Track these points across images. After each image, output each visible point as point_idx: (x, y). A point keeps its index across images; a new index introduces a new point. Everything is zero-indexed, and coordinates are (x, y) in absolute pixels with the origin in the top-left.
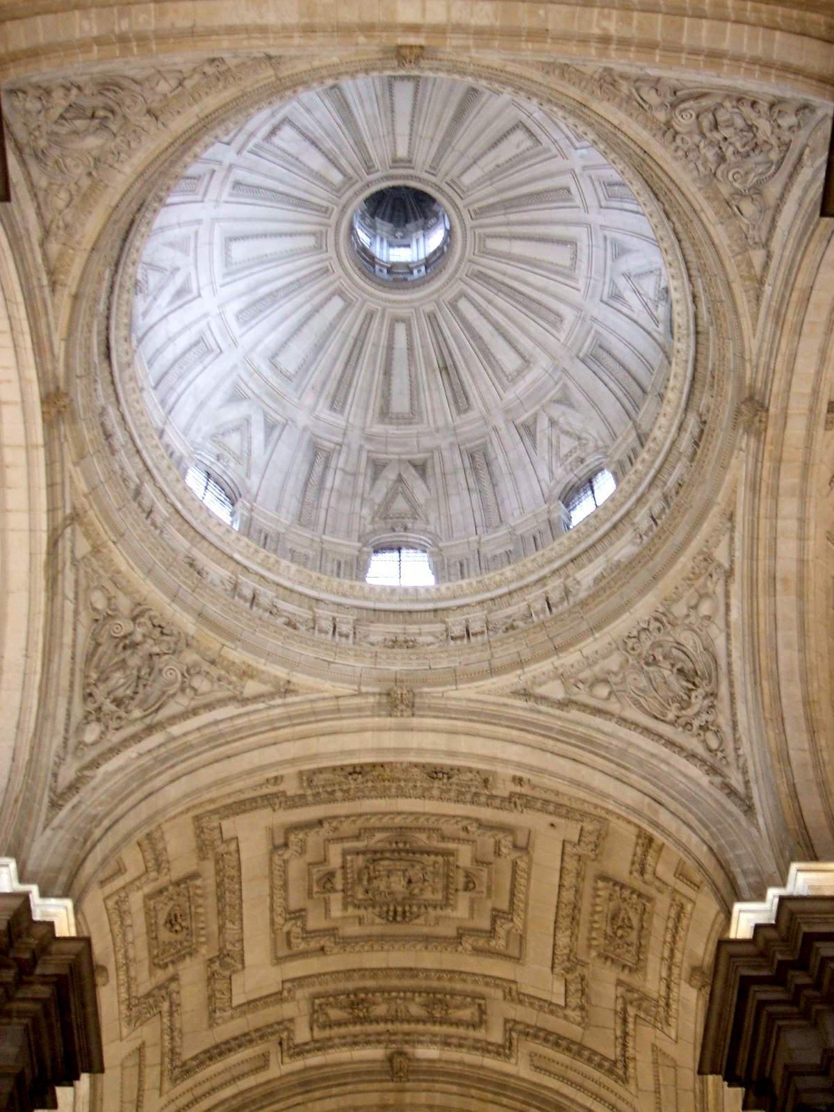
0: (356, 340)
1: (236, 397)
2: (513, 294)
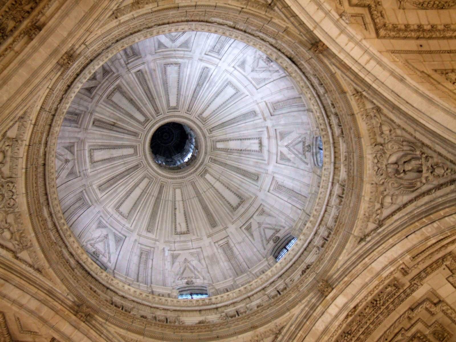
2: (121, 175)
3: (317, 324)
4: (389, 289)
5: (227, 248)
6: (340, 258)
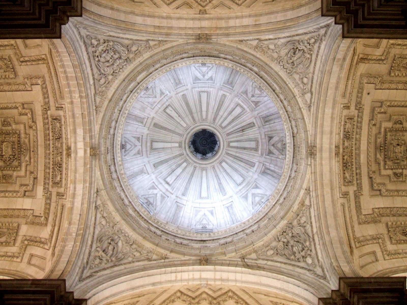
1: (246, 197)
3: (82, 131)
4: (58, 178)
5: (140, 120)
6: (99, 173)
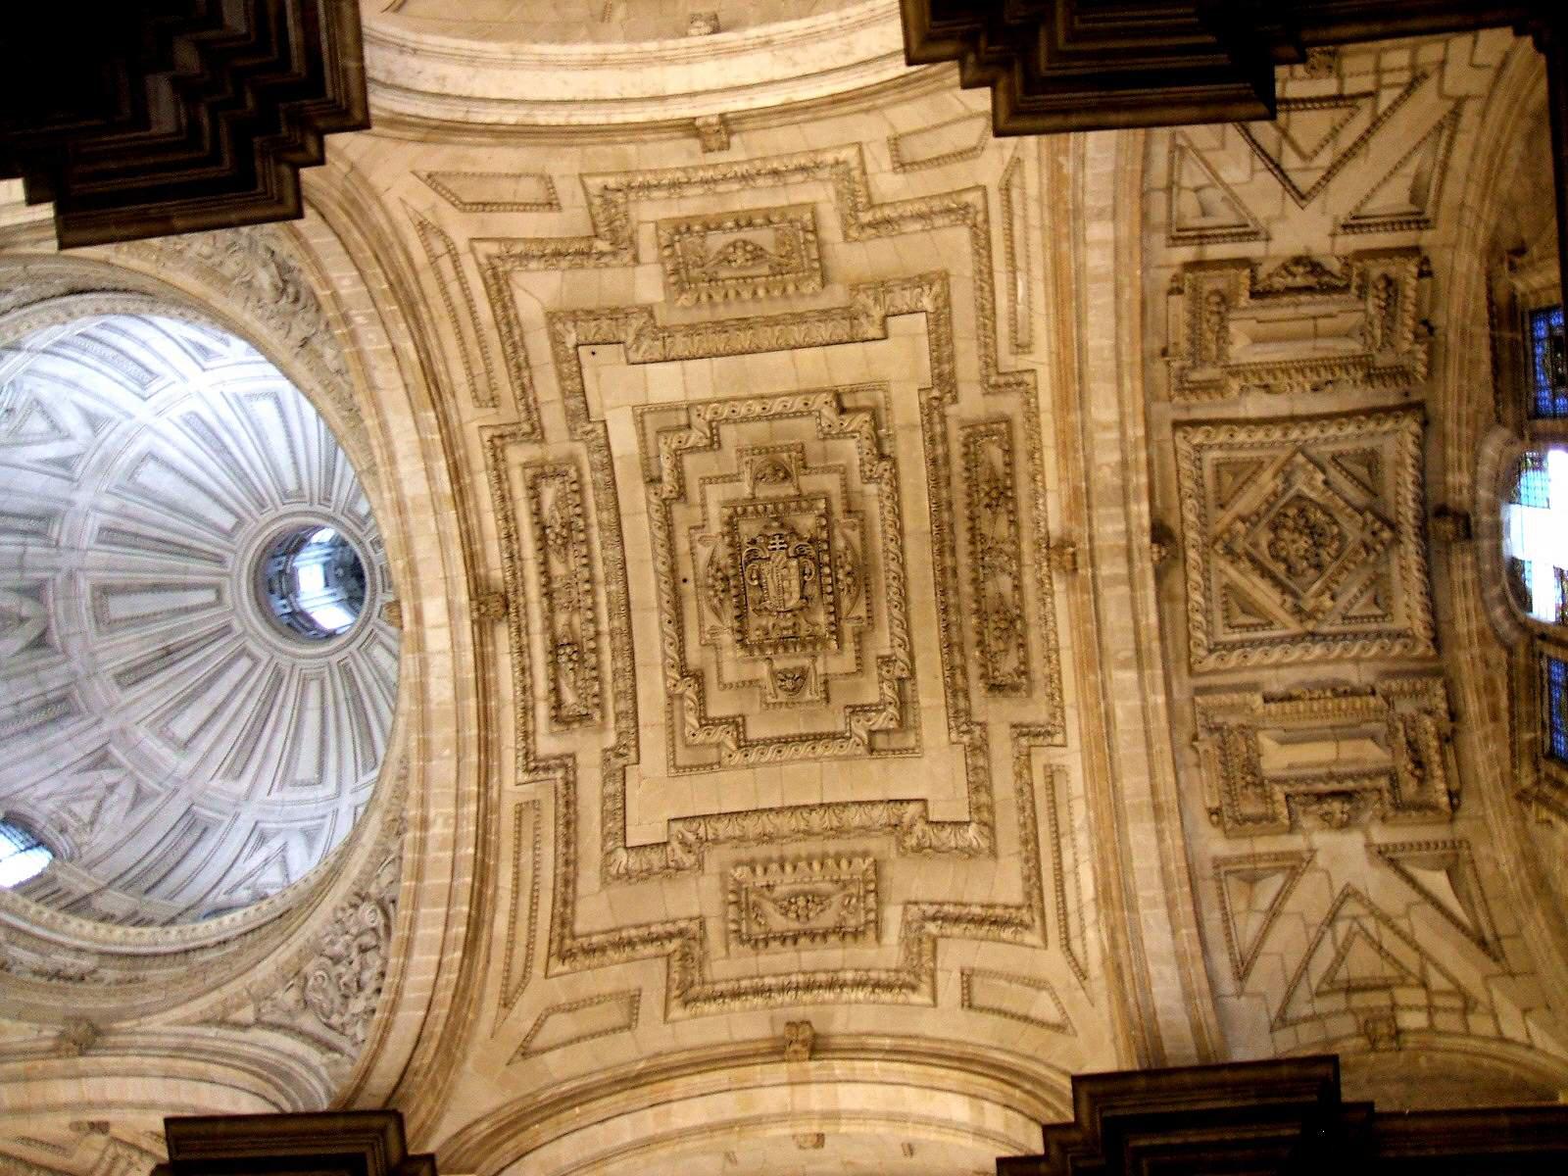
0: (188, 547)
1: (93, 421)
2: (262, 719)
4: (549, 493)
